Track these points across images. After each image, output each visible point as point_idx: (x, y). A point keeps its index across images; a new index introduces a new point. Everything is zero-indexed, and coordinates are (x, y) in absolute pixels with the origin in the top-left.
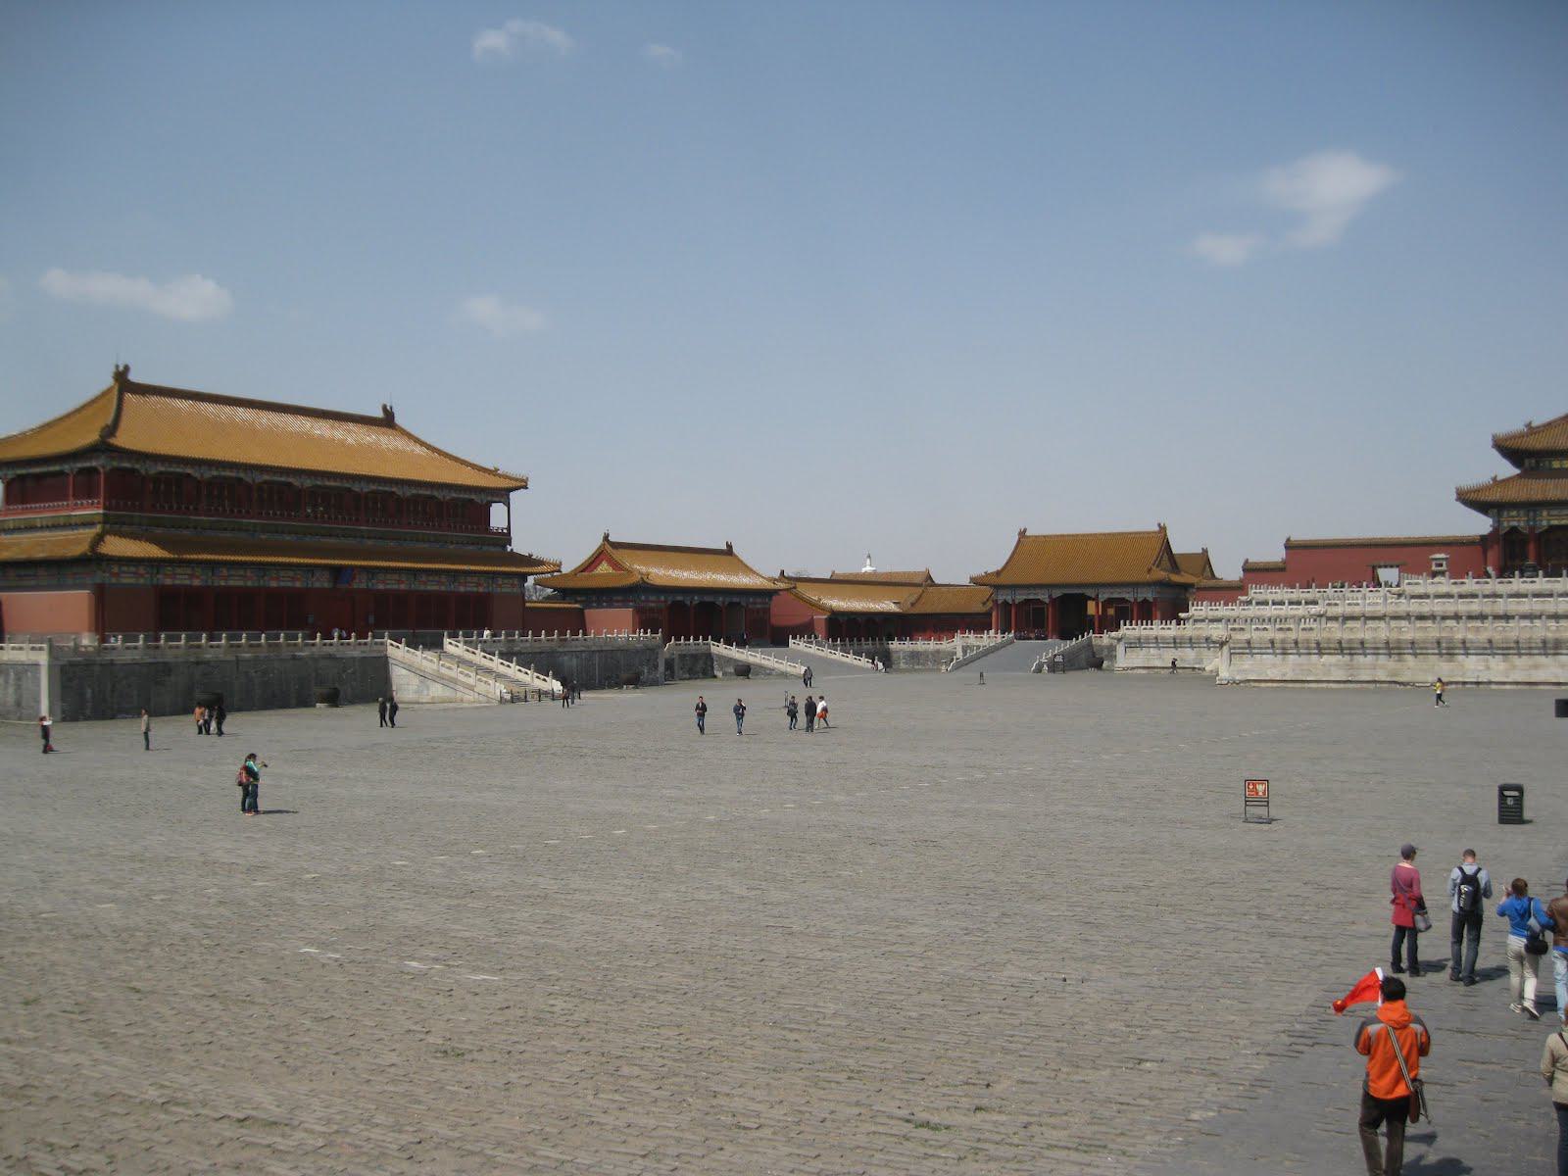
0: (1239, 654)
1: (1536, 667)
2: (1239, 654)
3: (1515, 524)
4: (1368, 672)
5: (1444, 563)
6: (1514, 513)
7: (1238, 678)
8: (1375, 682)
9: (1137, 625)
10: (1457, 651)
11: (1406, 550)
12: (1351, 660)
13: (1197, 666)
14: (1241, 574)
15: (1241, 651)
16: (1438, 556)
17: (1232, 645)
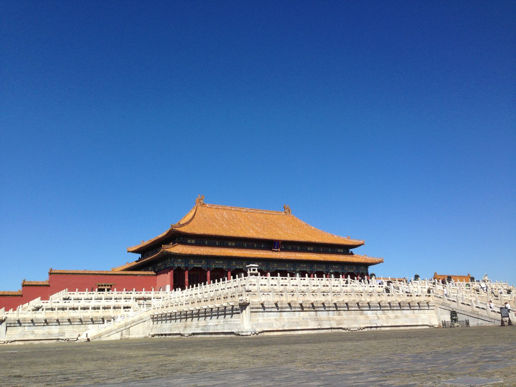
0: (255, 312)
1: (396, 317)
2: (255, 312)
3: (180, 265)
4: (327, 322)
5: (256, 269)
6: (180, 260)
7: (258, 330)
8: (332, 328)
9: (314, 277)
10: (365, 309)
11: (41, 287)
12: (316, 315)
13: (61, 338)
14: (20, 288)
15: (256, 310)
16: (254, 265)
17: (252, 306)
